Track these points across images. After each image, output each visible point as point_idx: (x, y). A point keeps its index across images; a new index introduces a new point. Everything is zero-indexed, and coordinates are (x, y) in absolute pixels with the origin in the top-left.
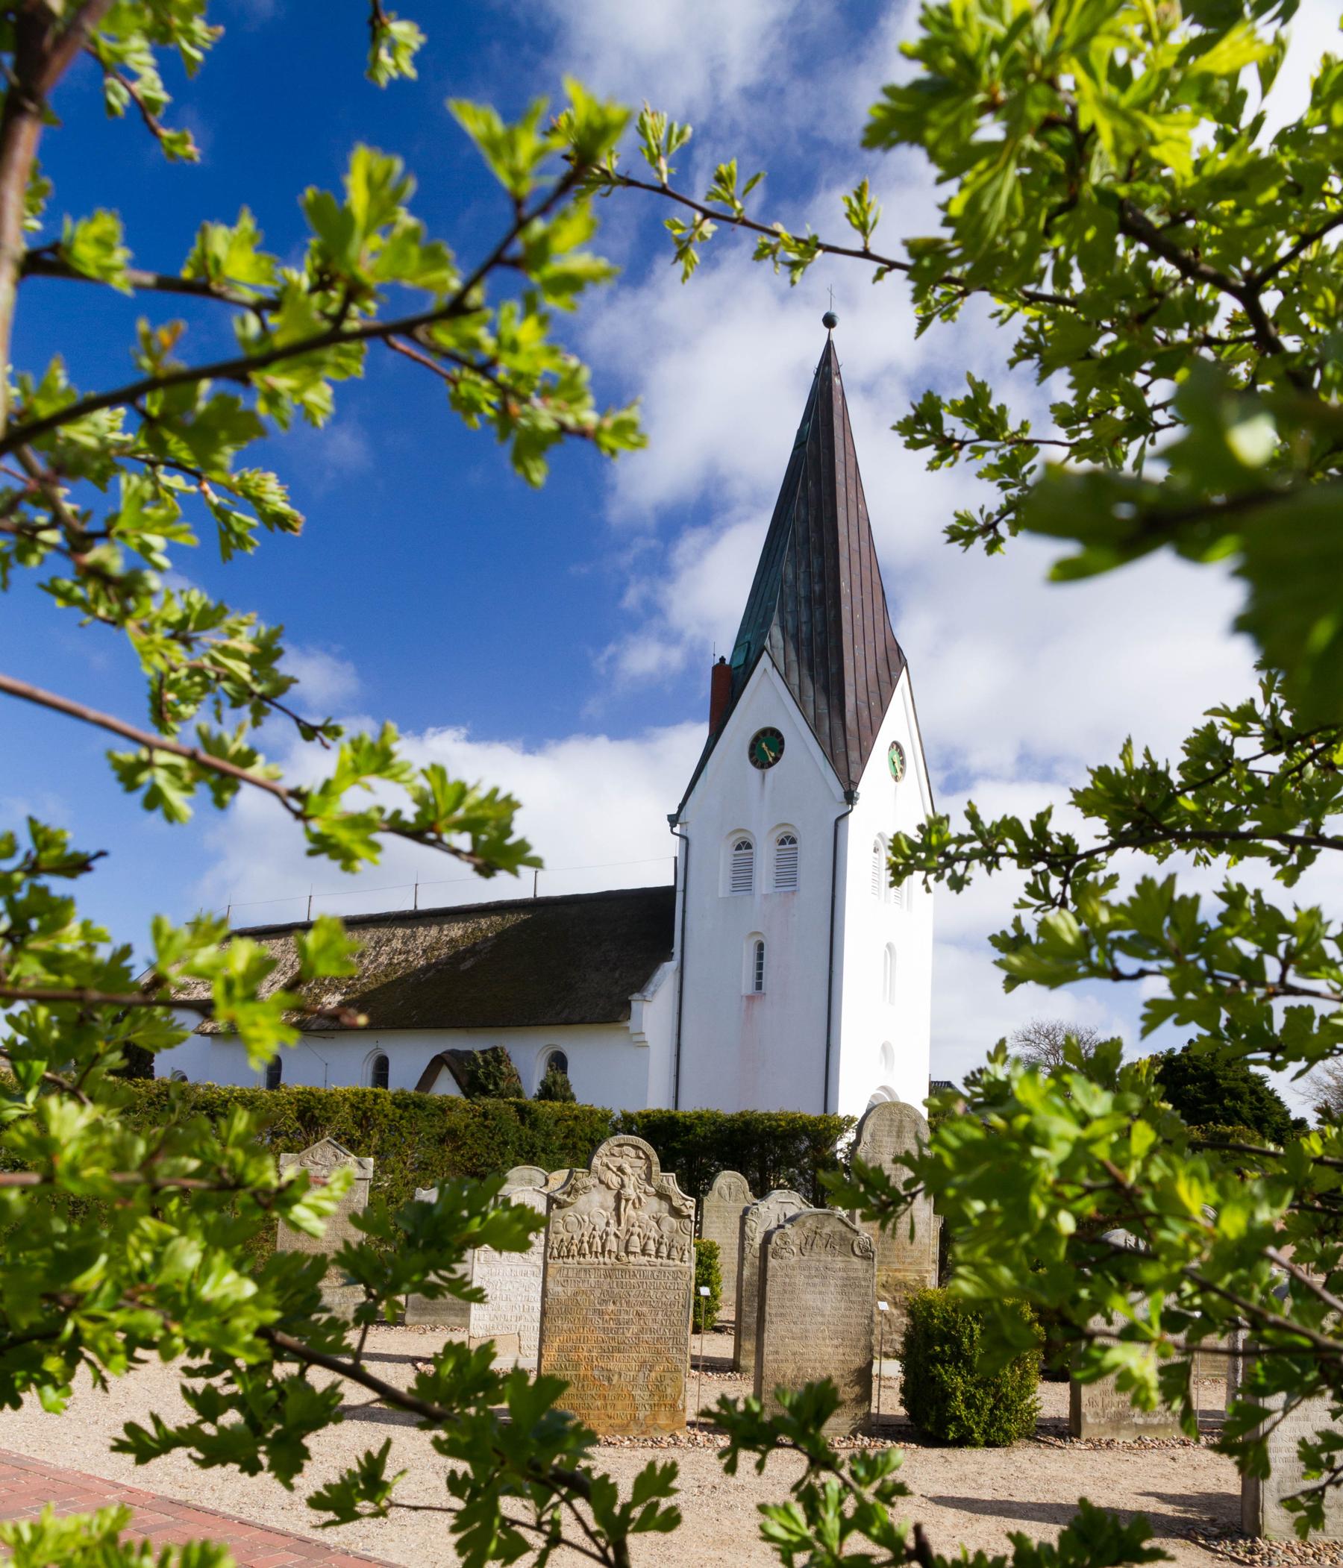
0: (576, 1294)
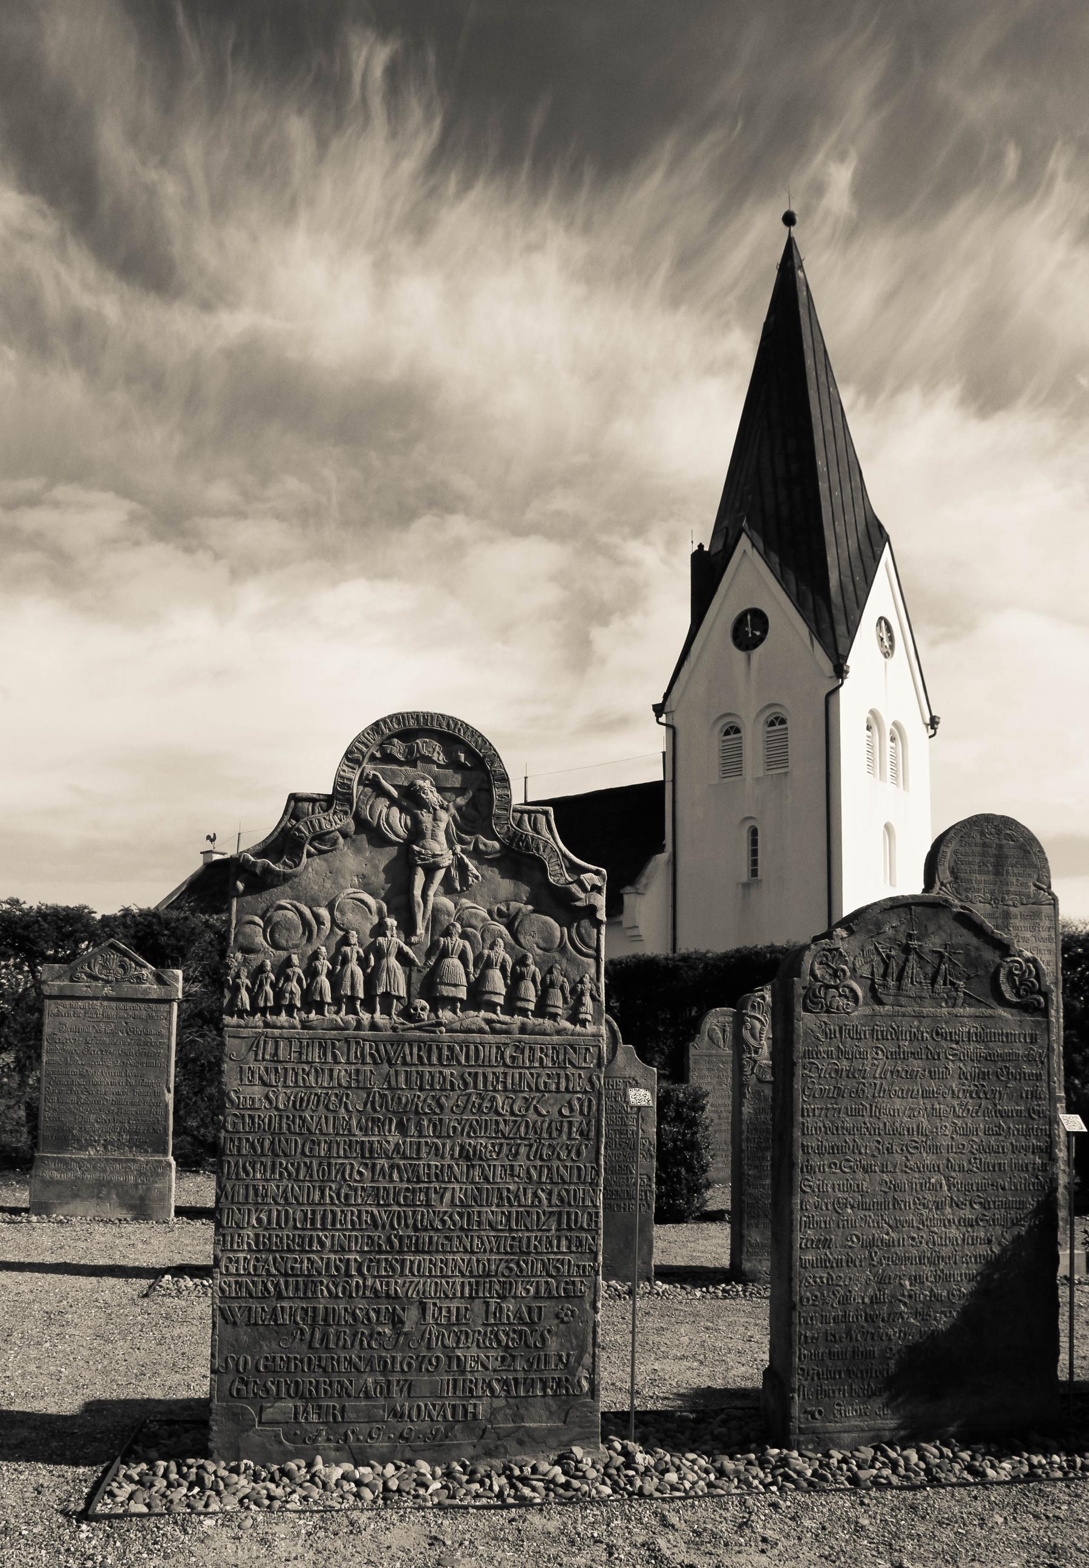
0: (298, 1105)
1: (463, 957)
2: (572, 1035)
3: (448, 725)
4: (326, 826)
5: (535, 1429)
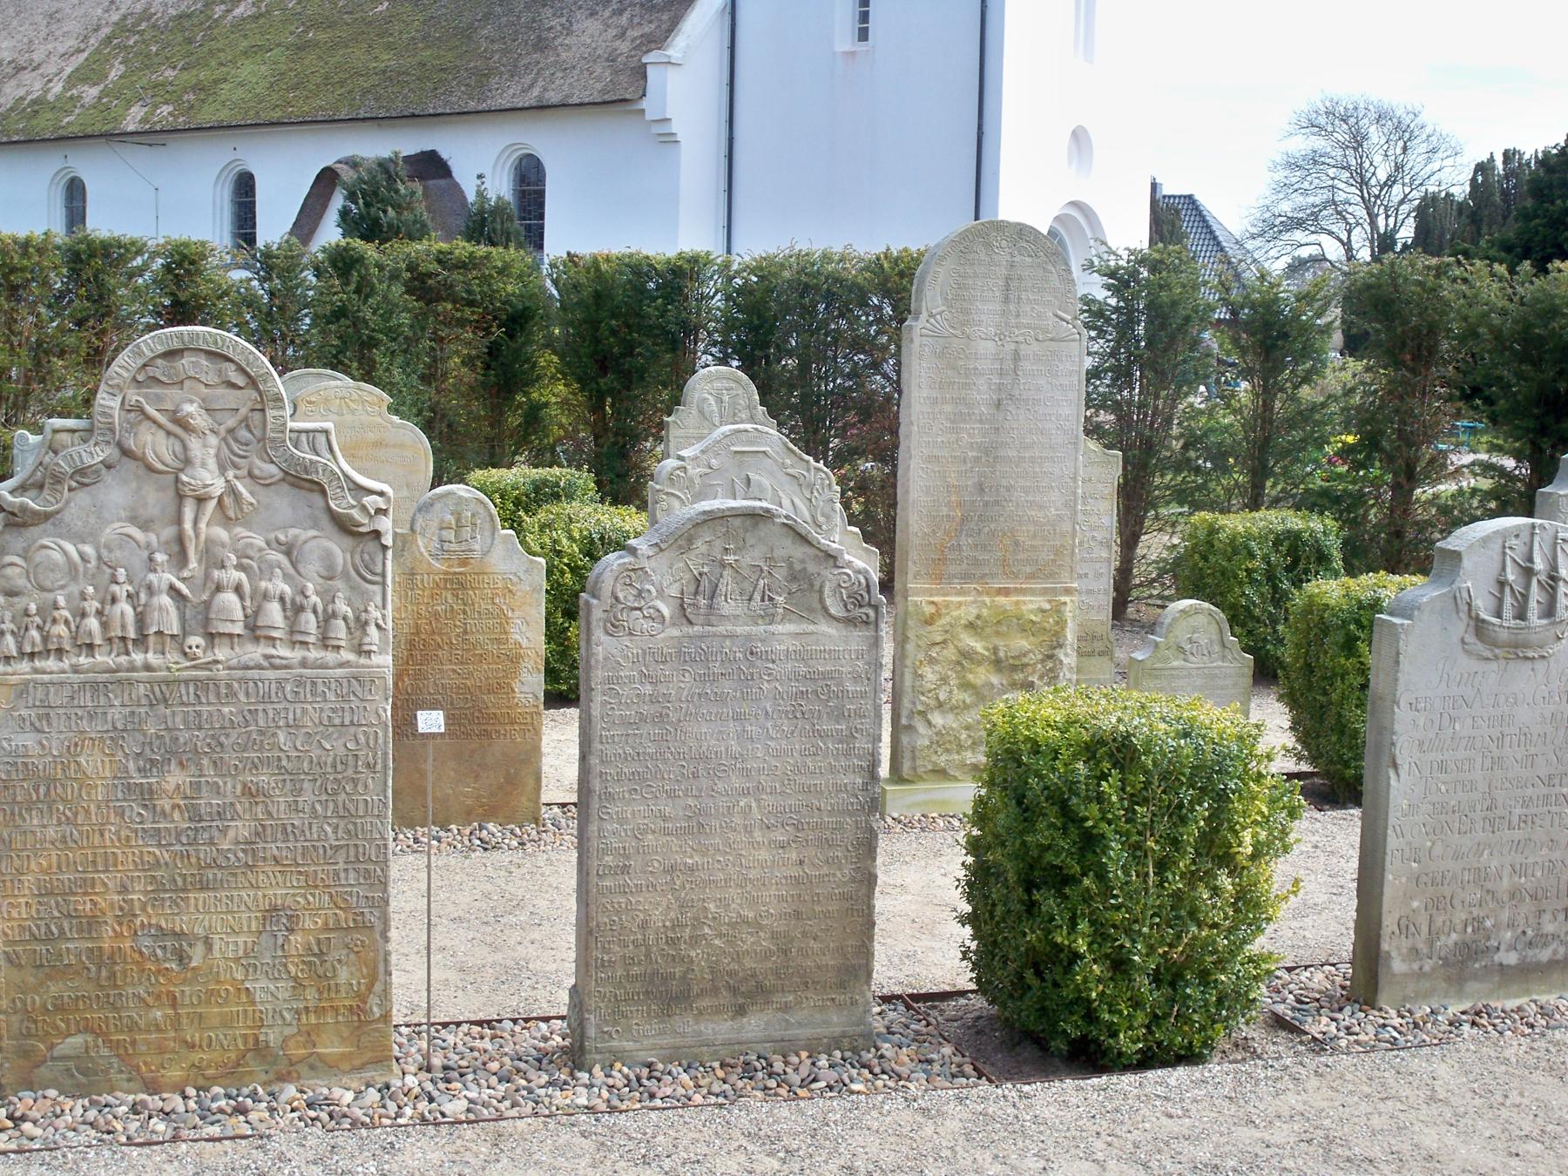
1: (238, 589)
2: (357, 667)
3: (216, 343)
4: (88, 461)
5: (328, 1054)
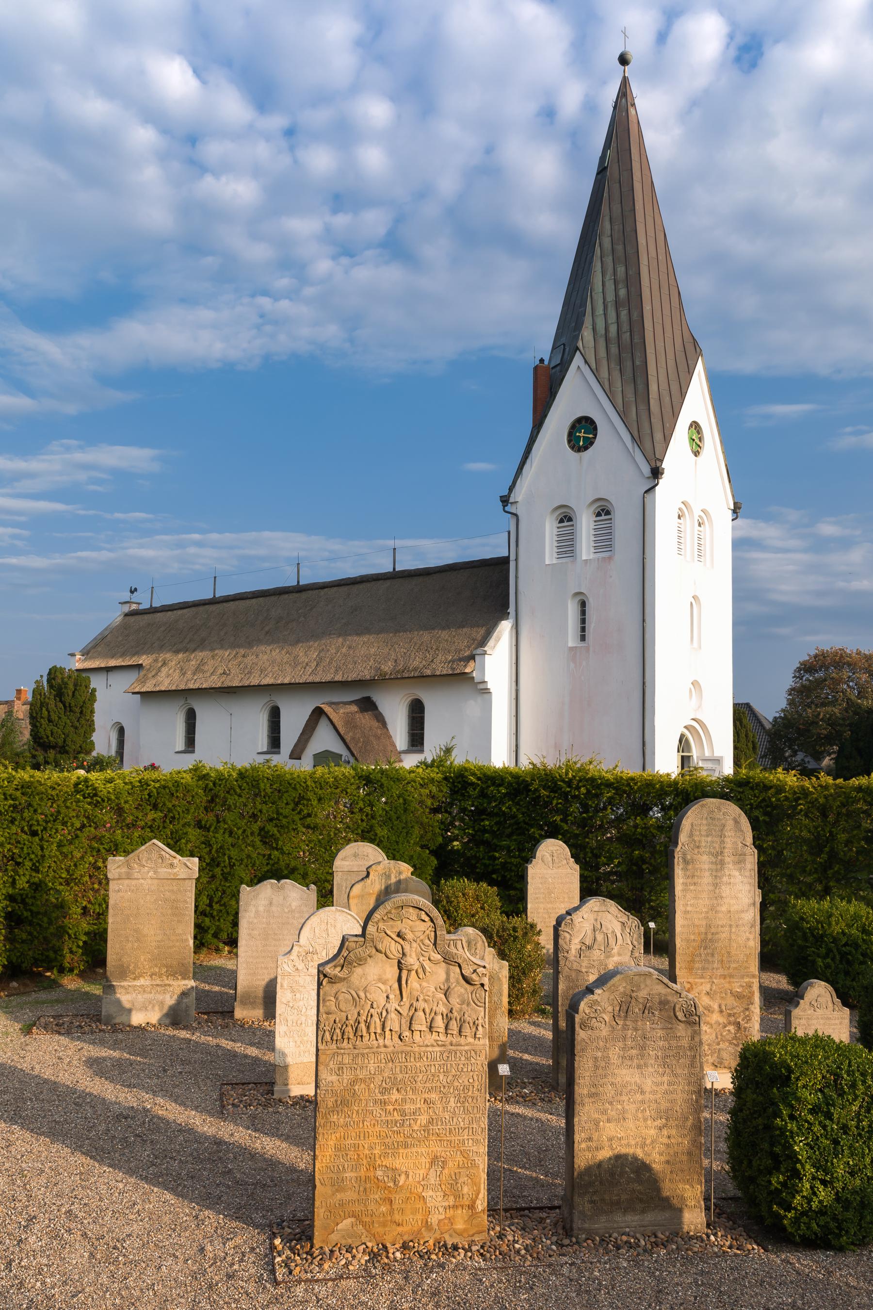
0: (353, 1082)
1: (424, 1010)
